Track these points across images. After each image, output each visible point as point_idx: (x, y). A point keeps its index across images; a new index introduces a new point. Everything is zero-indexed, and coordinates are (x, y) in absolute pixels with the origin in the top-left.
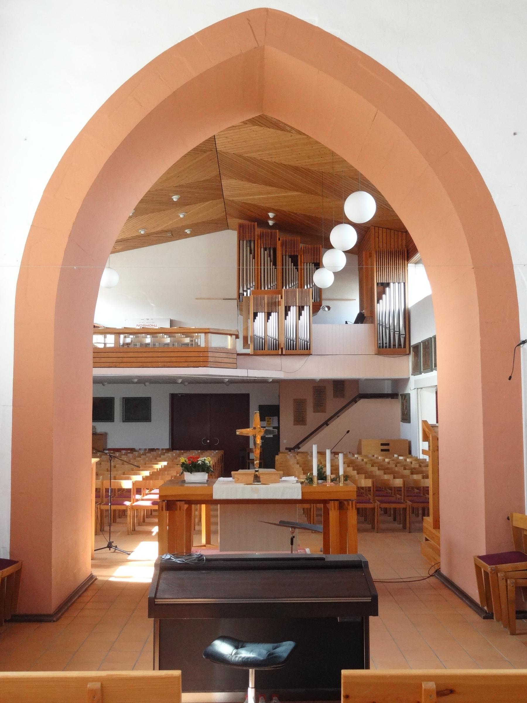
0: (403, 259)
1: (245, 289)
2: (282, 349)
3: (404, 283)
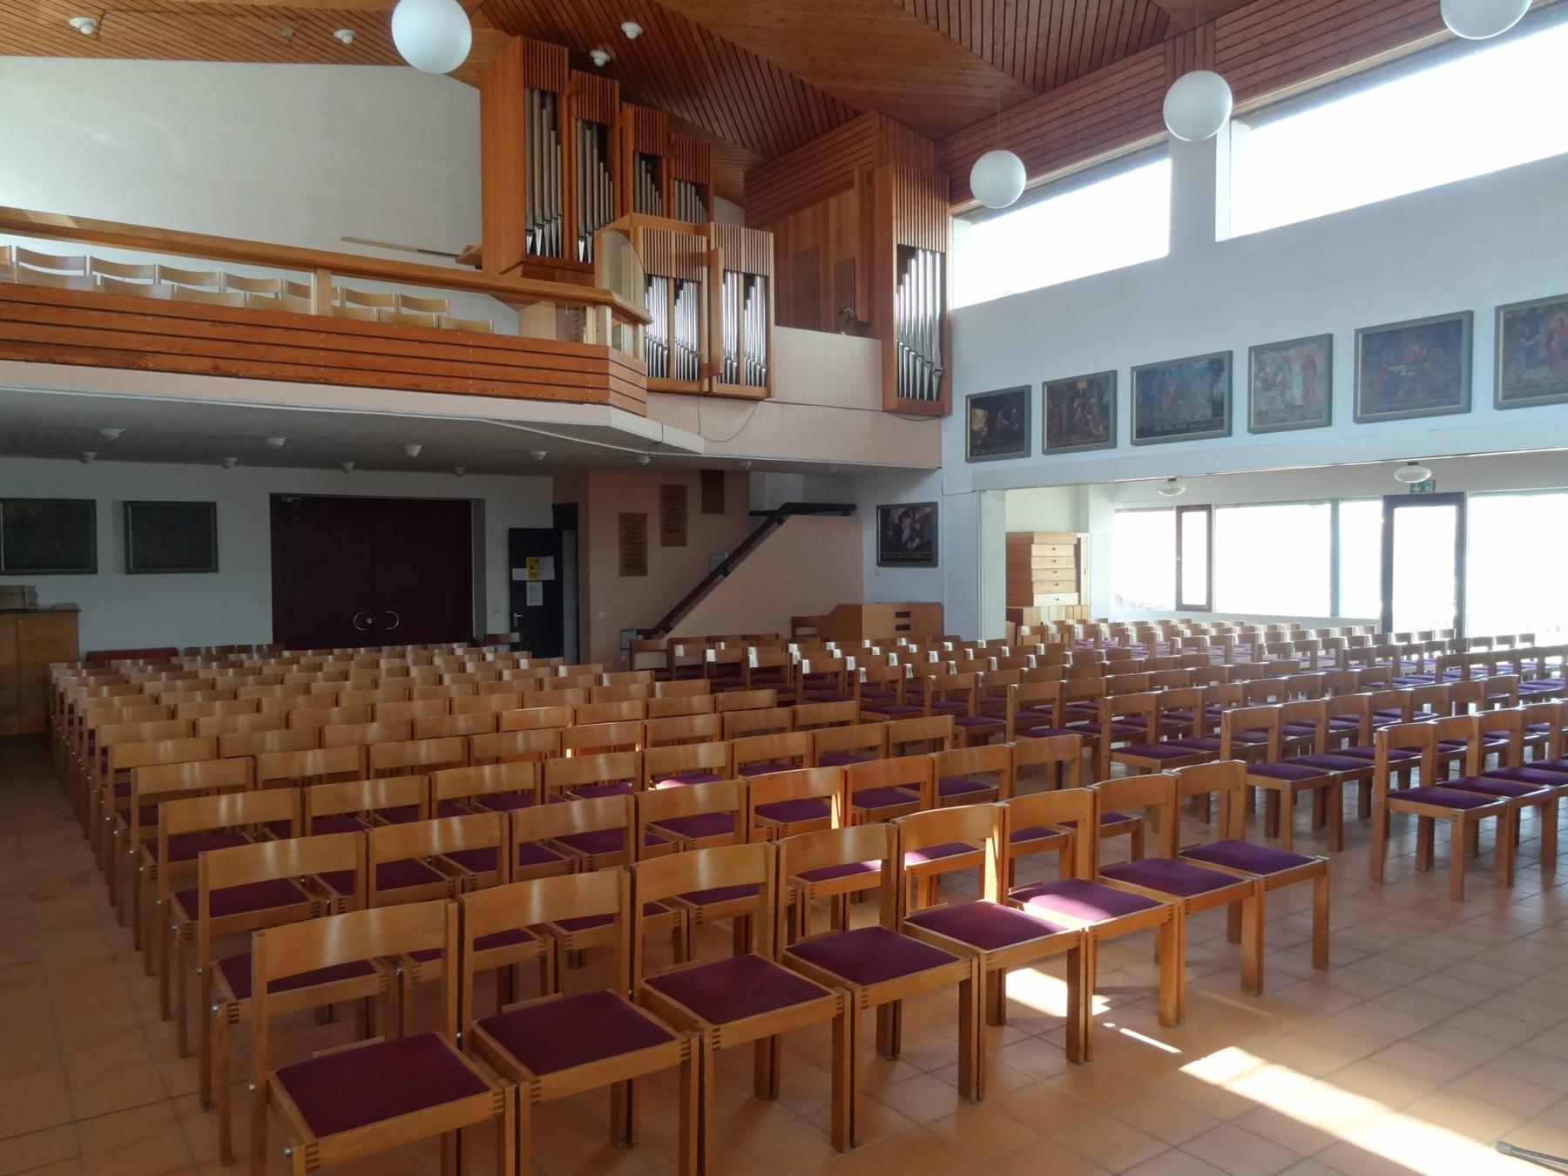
1: (539, 220)
3: (943, 256)
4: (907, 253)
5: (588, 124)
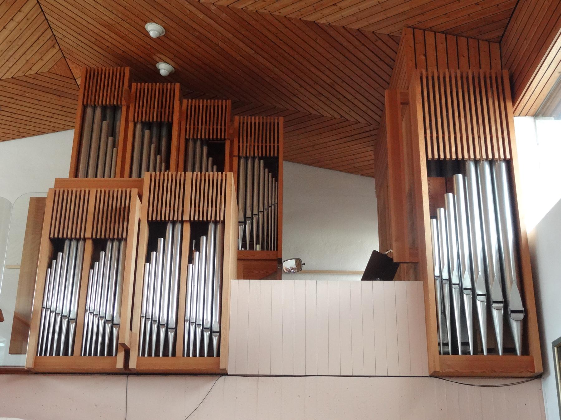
0: (501, 96)
2: (127, 352)
3: (509, 164)
4: (446, 171)
5: (148, 125)
